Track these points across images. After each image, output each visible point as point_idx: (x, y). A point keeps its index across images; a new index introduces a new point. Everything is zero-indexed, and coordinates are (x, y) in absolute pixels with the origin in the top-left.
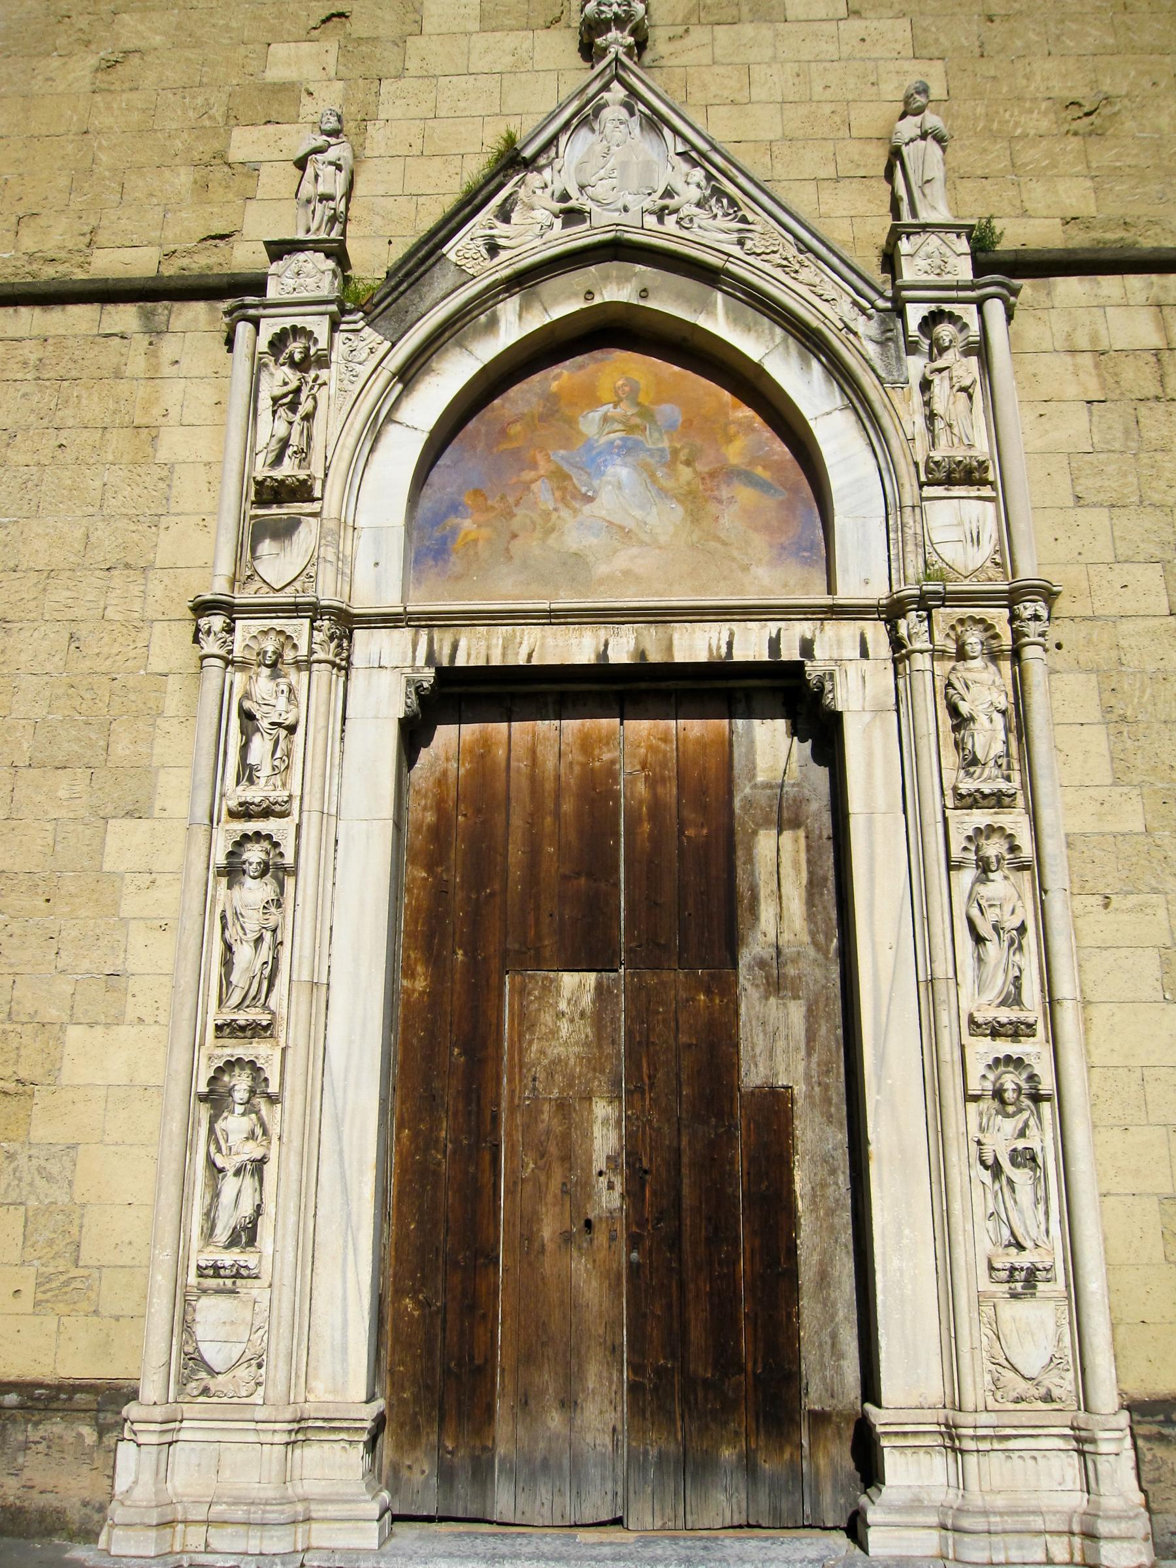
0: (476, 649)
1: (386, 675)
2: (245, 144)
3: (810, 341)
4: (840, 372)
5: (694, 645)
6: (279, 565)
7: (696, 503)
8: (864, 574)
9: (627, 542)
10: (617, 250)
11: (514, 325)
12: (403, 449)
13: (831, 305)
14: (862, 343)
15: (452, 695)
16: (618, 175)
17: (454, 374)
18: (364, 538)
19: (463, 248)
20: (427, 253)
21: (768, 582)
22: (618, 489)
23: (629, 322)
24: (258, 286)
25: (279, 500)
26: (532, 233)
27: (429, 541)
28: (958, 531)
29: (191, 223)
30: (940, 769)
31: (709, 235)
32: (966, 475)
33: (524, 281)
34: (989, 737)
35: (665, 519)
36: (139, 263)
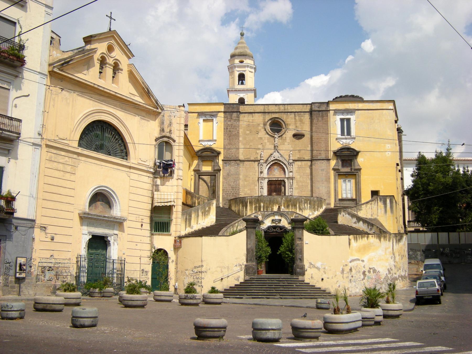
0: (270, 179)
1: (266, 181)
2: (258, 151)
3: (285, 164)
4: (286, 166)
5: (279, 179)
6: (262, 175)
7: (280, 172)
8: (287, 176)
9: (277, 174)
10: (276, 160)
11: (272, 163)
12: (267, 169)
13: (286, 163)
14: (287, 165)
15: (269, 181)
16: (276, 155)
17: (269, 166)
18: (265, 174)
19: (269, 159)
20: (267, 160)
21: (283, 176)
22: (276, 171)
23: (277, 163)
24: (259, 161)
25: (261, 172)
26: (272, 159)
27: (268, 174)
28: (291, 174)
29: (255, 157)
30: (289, 185)
31: (281, 159)
32: (291, 172)
33: (272, 161)
34: (291, 183)
35: (278, 172)
36: (252, 158)
